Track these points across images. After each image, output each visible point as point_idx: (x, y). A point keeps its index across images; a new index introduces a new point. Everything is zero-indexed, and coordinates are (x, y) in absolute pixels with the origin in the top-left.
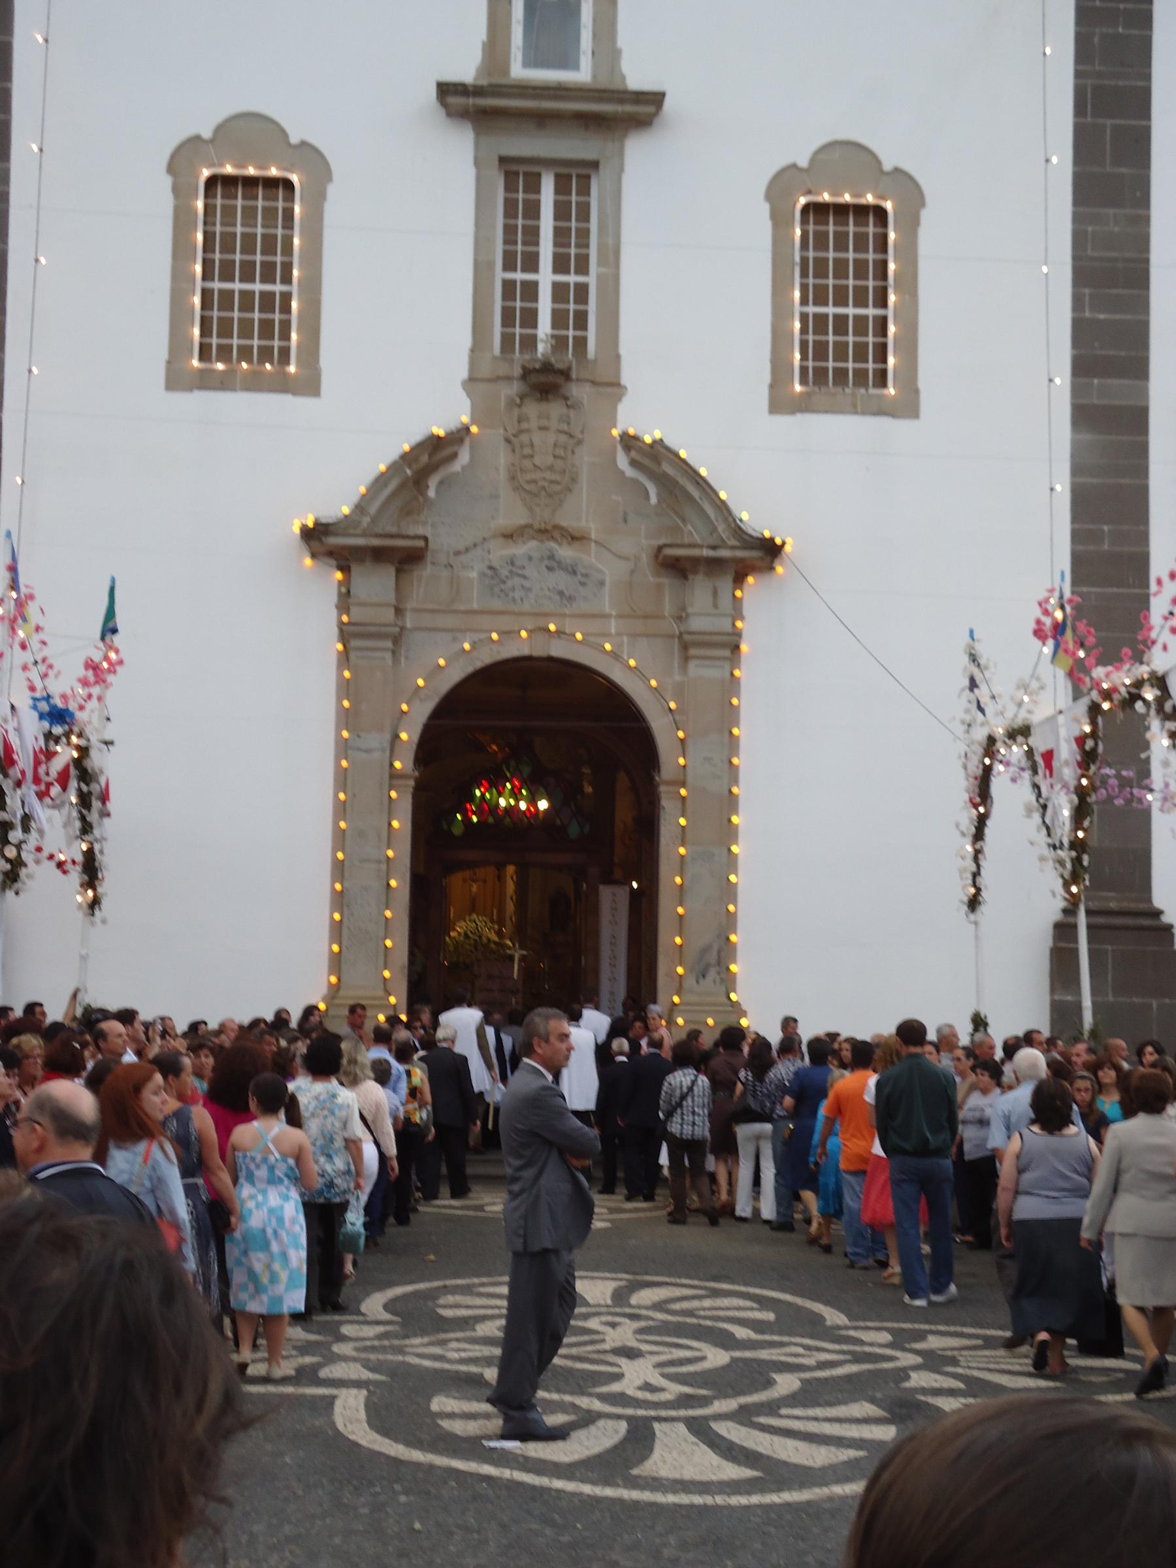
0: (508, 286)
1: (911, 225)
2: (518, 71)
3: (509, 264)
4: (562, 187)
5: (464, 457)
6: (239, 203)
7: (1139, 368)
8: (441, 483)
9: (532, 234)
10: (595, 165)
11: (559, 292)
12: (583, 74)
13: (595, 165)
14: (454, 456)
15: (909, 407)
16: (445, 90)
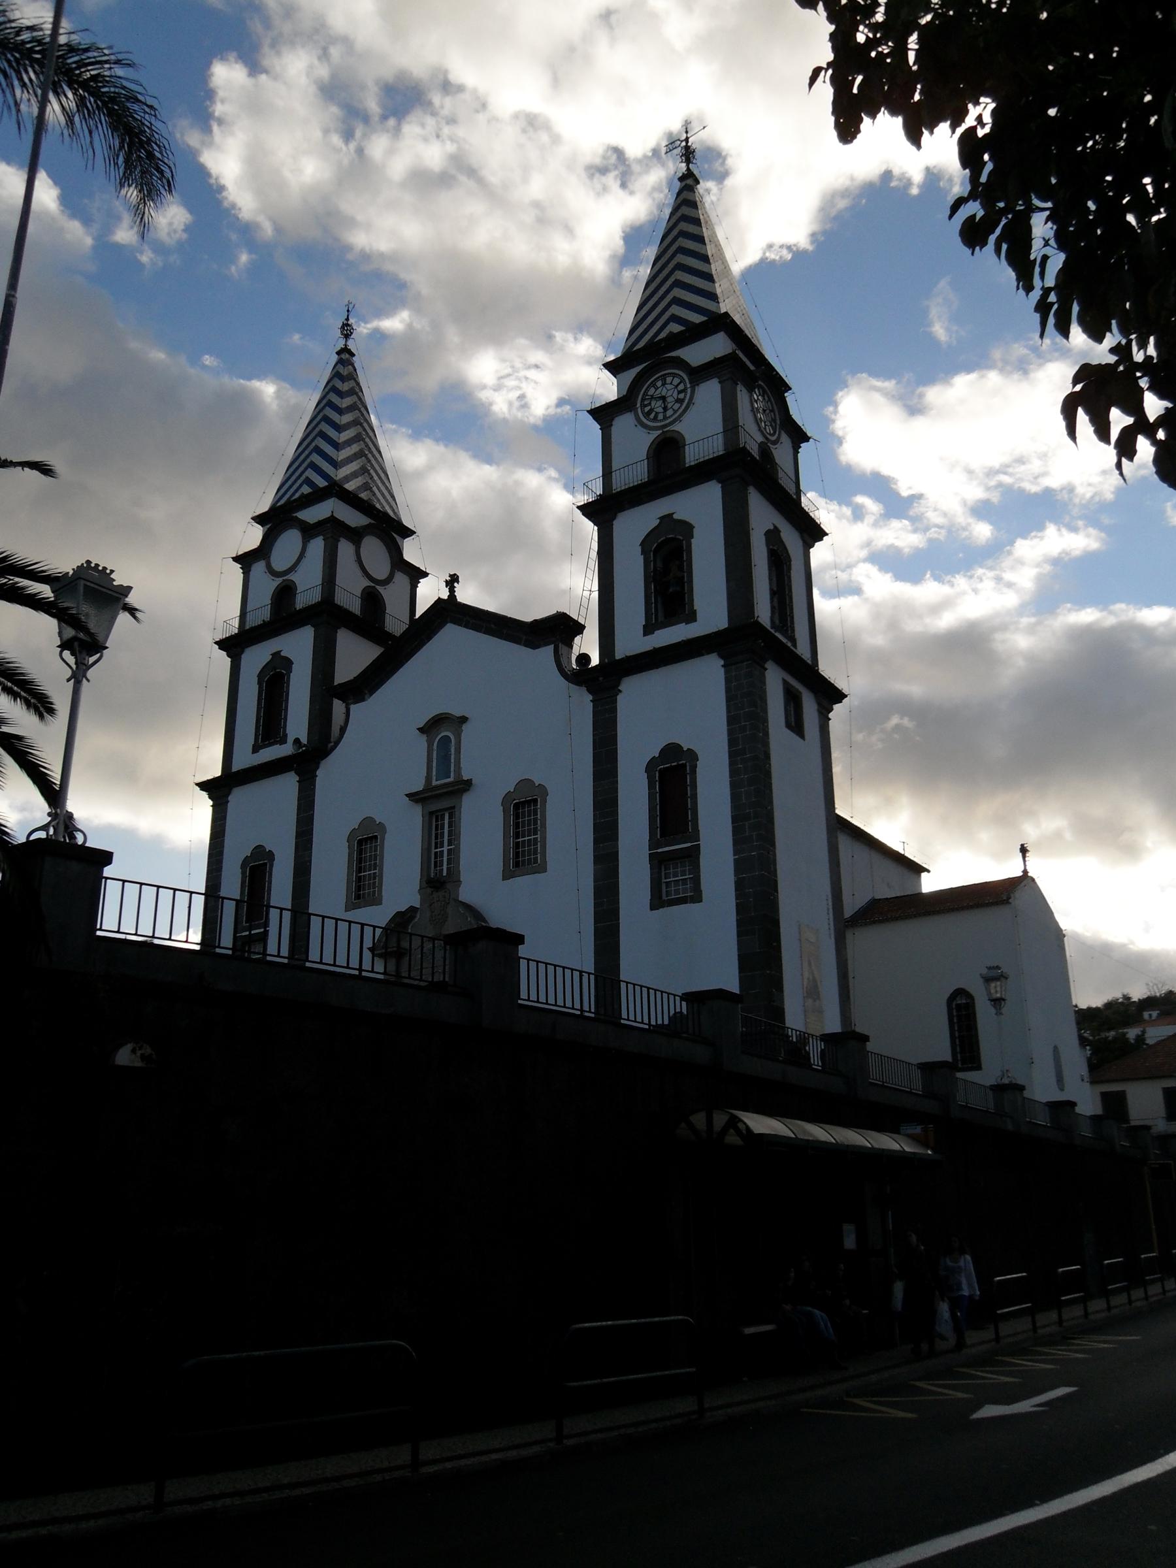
0: (436, 853)
1: (544, 802)
2: (434, 783)
3: (436, 848)
4: (450, 818)
5: (418, 916)
6: (373, 845)
7: (614, 836)
8: (412, 927)
9: (443, 834)
10: (454, 807)
11: (449, 851)
12: (451, 779)
13: (454, 807)
14: (414, 917)
15: (542, 869)
16: (410, 796)
